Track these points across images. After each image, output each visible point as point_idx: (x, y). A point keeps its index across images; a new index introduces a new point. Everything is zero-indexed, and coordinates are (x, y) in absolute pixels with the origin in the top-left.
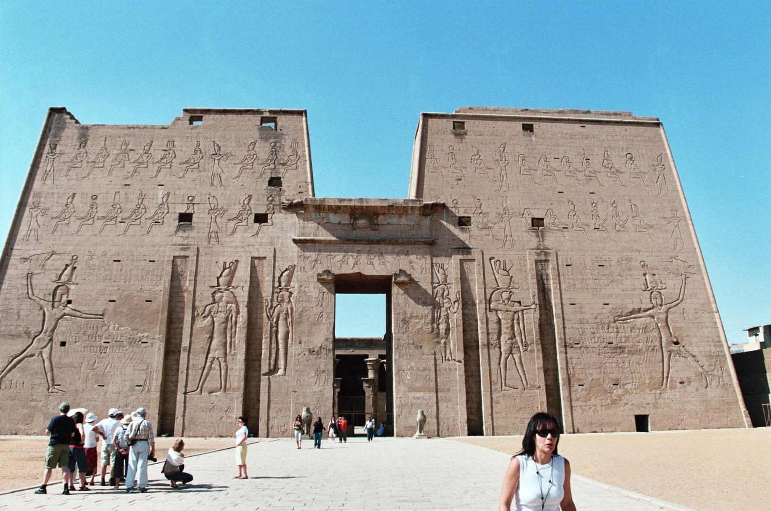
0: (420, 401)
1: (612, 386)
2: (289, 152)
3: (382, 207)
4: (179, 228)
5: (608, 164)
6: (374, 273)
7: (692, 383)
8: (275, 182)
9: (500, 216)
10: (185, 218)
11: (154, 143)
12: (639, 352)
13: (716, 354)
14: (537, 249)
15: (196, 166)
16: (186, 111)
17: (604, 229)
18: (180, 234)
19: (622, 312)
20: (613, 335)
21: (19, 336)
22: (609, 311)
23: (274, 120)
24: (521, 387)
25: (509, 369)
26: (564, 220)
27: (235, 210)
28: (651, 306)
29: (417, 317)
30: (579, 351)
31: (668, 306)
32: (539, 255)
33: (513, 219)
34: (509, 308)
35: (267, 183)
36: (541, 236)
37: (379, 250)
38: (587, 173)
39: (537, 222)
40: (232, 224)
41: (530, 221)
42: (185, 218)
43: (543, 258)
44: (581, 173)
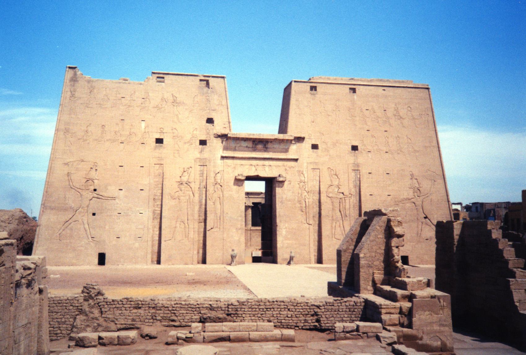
2: (216, 102)
4: (156, 147)
8: (210, 121)
9: (334, 144)
10: (159, 141)
11: (137, 93)
15: (162, 110)
16: (153, 73)
18: (157, 151)
21: (66, 210)
23: (207, 82)
26: (370, 148)
27: (188, 137)
28: (413, 197)
29: (289, 201)
35: (205, 122)
38: (384, 119)
39: (355, 148)
40: (186, 146)
41: (350, 147)
42: (159, 141)
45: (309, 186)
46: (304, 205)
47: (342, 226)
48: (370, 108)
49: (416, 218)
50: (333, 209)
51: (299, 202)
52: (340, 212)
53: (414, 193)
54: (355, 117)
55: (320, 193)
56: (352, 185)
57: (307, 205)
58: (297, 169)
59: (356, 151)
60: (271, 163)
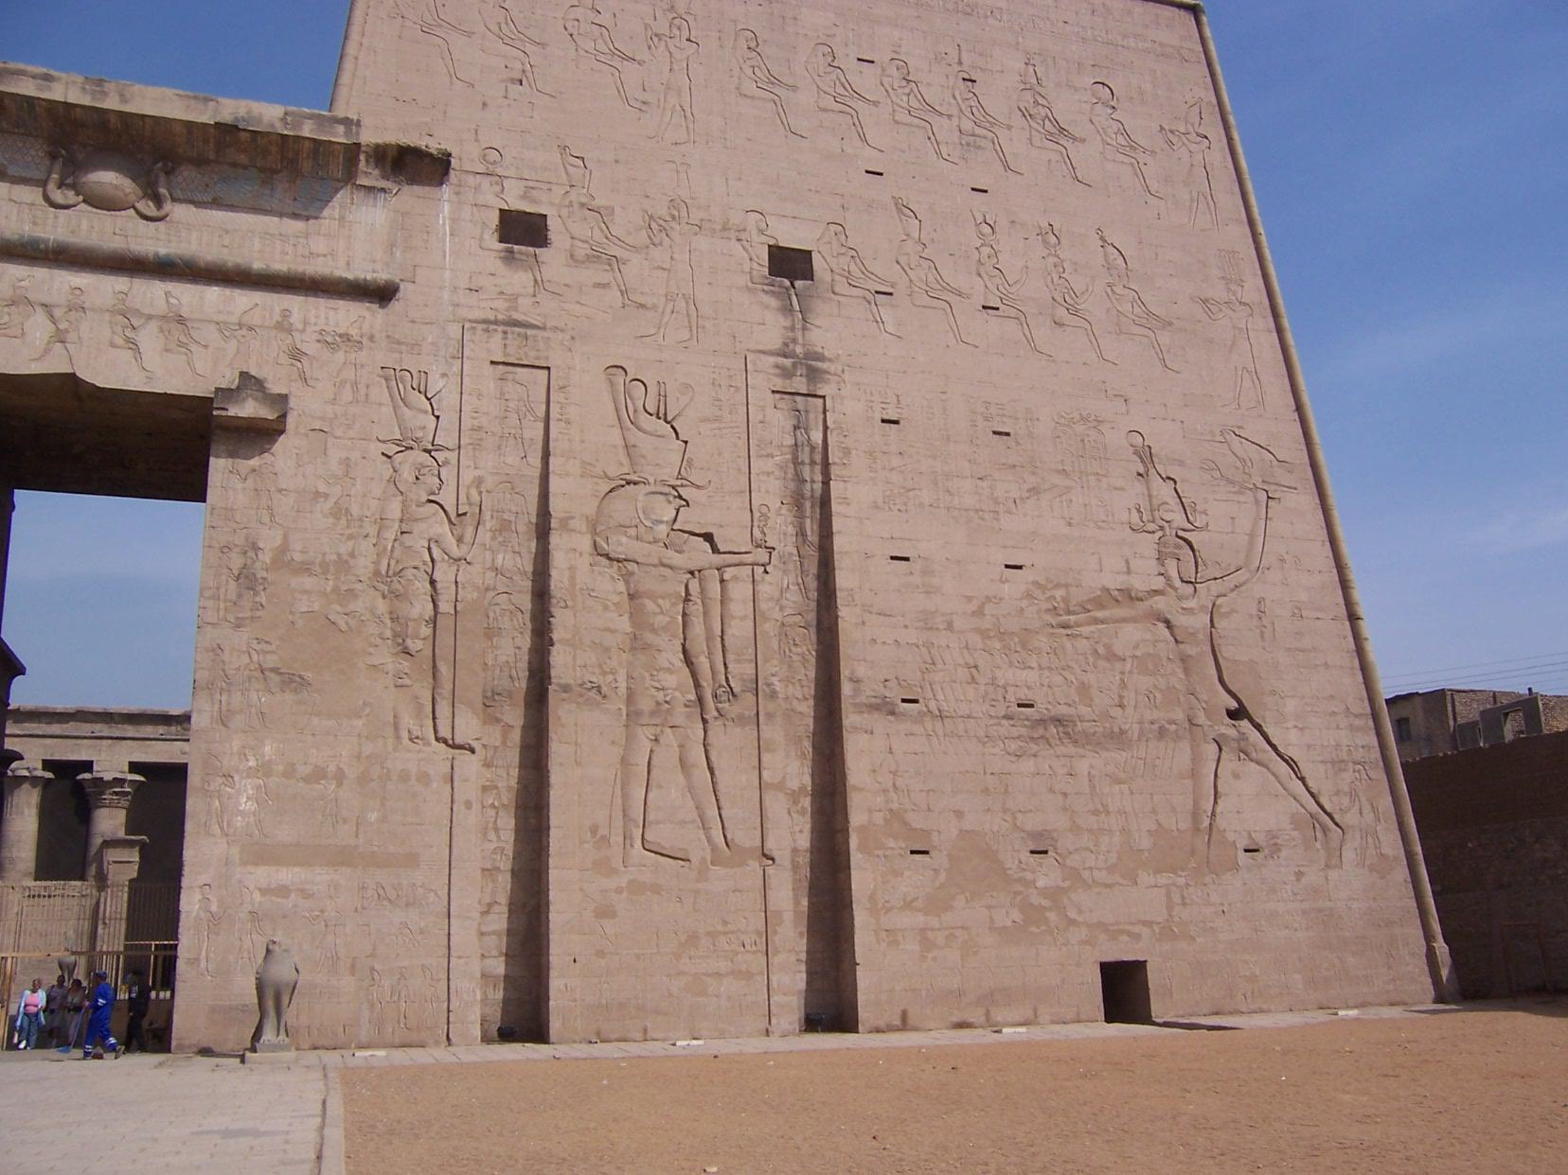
0: (288, 903)
1: (1025, 856)
3: (190, 125)
5: (1036, 102)
6: (136, 383)
7: (1283, 854)
9: (656, 227)
12: (1119, 738)
13: (1359, 754)
14: (785, 356)
17: (1013, 313)
19: (1066, 600)
20: (1032, 677)
22: (1023, 587)
24: (699, 852)
25: (660, 787)
28: (1159, 583)
29: (305, 568)
30: (918, 729)
31: (1216, 587)
32: (787, 374)
33: (702, 243)
34: (676, 559)
36: (799, 313)
37: (167, 294)
38: (967, 125)
39: (789, 265)
43: (800, 384)
44: (945, 121)
45: (467, 476)
46: (422, 608)
47: (697, 754)
48: (882, 56)
49: (1179, 715)
50: (637, 644)
51: (389, 581)
52: (688, 661)
53: (1160, 560)
54: (794, 88)
55: (543, 530)
56: (771, 492)
57: (445, 607)
58: (383, 356)
59: (798, 283)
60: (187, 295)
